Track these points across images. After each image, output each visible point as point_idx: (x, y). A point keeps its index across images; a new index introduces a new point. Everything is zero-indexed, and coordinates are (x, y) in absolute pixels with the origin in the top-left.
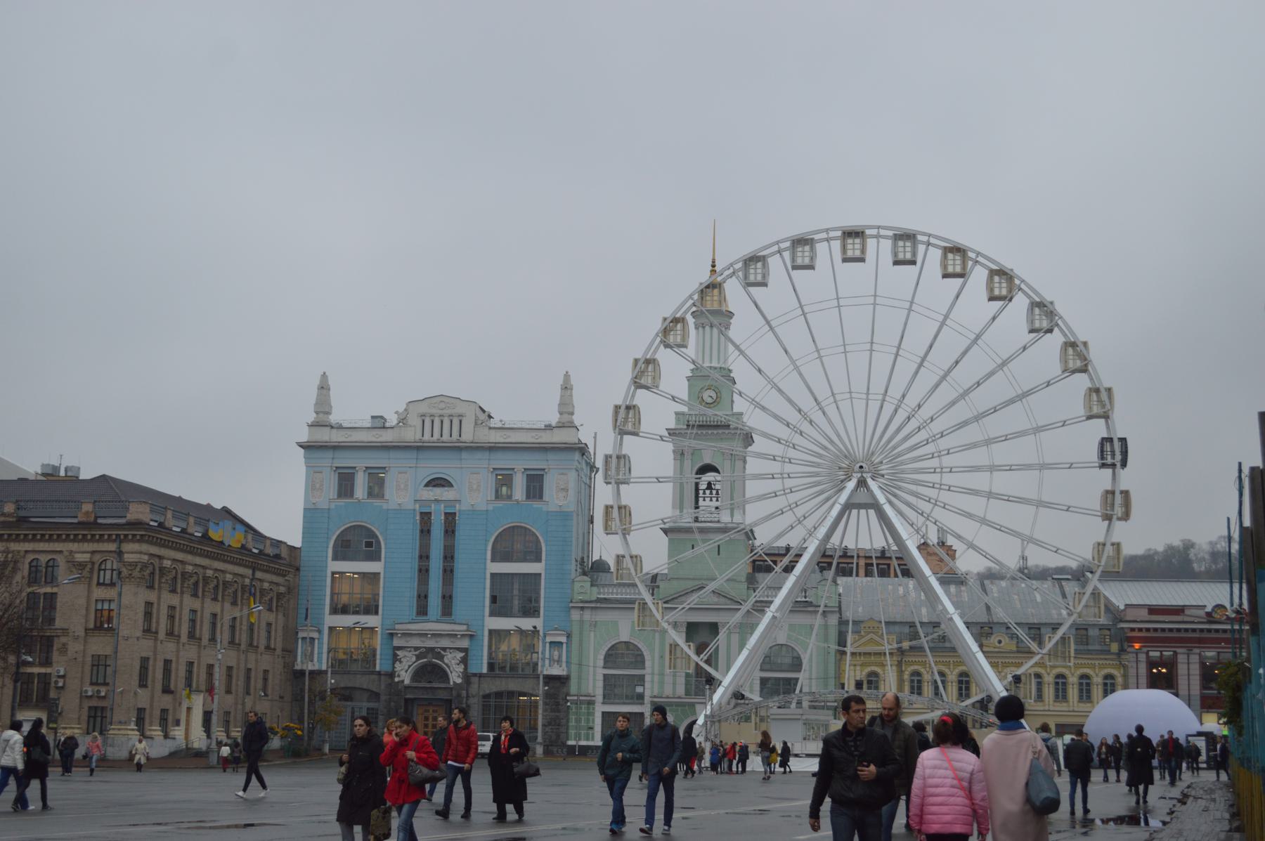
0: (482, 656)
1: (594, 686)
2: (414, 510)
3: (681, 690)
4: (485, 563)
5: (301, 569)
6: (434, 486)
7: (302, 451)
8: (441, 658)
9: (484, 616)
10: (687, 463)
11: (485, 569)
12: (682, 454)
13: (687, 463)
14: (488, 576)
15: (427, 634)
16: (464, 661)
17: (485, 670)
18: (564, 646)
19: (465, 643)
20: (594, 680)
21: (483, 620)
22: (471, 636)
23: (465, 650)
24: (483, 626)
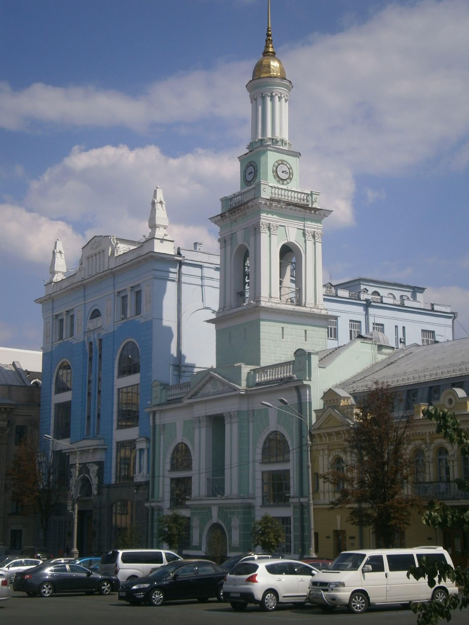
0: (111, 468)
1: (163, 492)
2: (84, 342)
3: (203, 492)
4: (113, 381)
5: (41, 404)
6: (95, 318)
7: (40, 306)
8: (88, 471)
9: (112, 430)
10: (228, 248)
11: (113, 386)
12: (225, 241)
13: (228, 248)
14: (116, 392)
15: (90, 450)
16: (100, 474)
17: (113, 481)
18: (146, 452)
19: (99, 457)
20: (164, 485)
21: (112, 434)
22: (105, 449)
23: (100, 464)
24: (112, 439)
